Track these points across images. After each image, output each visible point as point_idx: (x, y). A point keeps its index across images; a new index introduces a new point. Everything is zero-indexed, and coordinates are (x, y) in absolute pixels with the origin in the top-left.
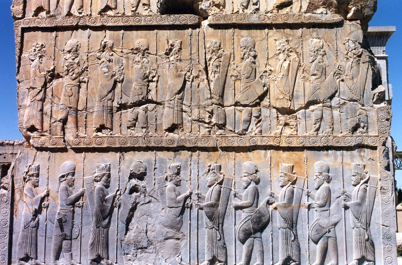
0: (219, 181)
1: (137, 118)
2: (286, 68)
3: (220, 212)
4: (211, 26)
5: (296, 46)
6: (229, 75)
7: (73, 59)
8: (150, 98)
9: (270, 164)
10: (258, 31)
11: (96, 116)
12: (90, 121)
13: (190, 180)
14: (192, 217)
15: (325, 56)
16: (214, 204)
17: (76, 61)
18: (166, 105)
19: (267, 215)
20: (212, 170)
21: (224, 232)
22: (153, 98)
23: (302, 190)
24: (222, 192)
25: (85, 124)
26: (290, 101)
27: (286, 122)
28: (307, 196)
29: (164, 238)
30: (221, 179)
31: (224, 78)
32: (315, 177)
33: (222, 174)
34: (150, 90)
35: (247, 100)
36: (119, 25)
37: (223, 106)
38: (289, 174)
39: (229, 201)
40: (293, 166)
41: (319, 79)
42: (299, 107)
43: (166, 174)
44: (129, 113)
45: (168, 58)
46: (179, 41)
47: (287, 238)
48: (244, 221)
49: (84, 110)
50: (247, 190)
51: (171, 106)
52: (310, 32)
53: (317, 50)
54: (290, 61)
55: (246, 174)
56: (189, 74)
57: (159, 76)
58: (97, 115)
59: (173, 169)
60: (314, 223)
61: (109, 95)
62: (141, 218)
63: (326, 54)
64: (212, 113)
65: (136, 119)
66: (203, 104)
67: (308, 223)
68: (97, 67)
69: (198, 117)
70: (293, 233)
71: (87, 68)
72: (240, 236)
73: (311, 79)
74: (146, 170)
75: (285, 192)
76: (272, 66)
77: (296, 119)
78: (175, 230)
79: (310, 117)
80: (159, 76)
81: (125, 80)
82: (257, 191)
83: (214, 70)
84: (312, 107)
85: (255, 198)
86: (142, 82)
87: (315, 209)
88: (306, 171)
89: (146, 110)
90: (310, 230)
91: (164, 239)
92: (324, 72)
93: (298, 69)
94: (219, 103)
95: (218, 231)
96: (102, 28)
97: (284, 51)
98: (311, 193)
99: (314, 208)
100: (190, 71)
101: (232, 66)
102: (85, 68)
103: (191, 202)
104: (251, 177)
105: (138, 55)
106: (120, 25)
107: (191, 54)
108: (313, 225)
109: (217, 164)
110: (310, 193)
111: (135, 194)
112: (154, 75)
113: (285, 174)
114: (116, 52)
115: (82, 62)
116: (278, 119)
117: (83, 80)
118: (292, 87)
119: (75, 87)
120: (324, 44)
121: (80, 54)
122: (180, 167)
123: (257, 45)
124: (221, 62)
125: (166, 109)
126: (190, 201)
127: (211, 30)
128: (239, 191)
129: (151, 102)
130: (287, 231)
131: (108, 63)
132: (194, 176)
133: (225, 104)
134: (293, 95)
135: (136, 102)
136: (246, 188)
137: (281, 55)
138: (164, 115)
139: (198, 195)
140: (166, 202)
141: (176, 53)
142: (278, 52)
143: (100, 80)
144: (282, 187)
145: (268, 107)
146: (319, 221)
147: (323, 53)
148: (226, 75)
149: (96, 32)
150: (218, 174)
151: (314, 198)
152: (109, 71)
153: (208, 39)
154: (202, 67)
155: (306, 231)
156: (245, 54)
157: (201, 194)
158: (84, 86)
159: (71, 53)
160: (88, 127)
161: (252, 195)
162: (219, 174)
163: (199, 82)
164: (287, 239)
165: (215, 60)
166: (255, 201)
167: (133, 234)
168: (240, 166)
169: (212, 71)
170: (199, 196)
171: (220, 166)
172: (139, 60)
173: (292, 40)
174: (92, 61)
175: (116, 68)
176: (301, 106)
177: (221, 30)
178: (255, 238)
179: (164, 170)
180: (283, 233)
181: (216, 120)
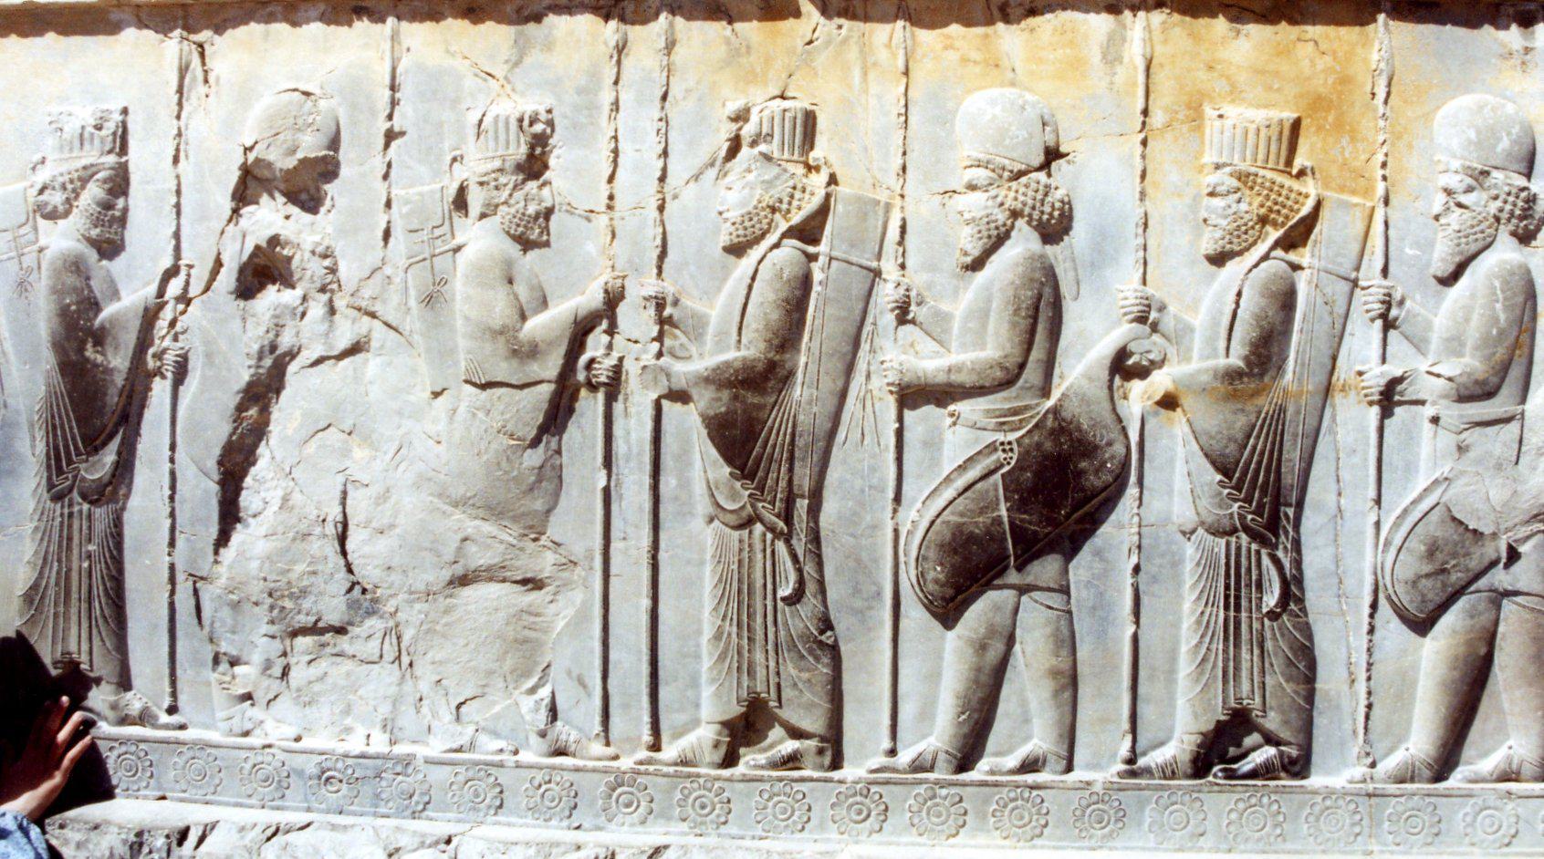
0: (796, 218)
3: (801, 418)
9: (1140, 105)
13: (610, 207)
14: (620, 447)
16: (760, 367)
19: (1110, 444)
20: (754, 144)
21: (827, 551)
23: (1346, 287)
24: (816, 288)
28: (1379, 323)
29: (446, 574)
30: (811, 204)
32: (1442, 198)
33: (817, 169)
38: (1269, 174)
39: (865, 346)
40: (1296, 126)
43: (461, 173)
47: (1238, 598)
48: (961, 482)
50: (981, 277)
55: (981, 175)
59: (502, 136)
60: (1415, 502)
62: (312, 447)
67: (1378, 501)
70: (1277, 563)
72: (931, 575)
74: (334, 143)
75: (1239, 294)
78: (516, 530)
82: (1047, 291)
85: (1032, 332)
87: (1429, 411)
88: (1380, 158)
90: (1387, 543)
91: (451, 583)
95: (788, 542)
98: (1408, 303)
99: (1422, 403)
103: (615, 355)
104: (1013, 195)
108: (1406, 511)
109: (787, 104)
110: (1401, 303)
111: (272, 297)
113: (1242, 177)
122: (550, 123)
126: (610, 347)
128: (930, 286)
130: (1239, 548)
132: (636, 183)
136: (977, 265)
139: (660, 306)
140: (453, 351)
144: (1219, 259)
146: (1451, 492)
150: (792, 168)
151: (1426, 341)
155: (1361, 554)
157: (676, 303)
161: (1016, 312)
162: (800, 170)
164: (1233, 601)
166: (1037, 354)
167: (262, 547)
168: (945, 119)
170: (667, 312)
171: (810, 120)
178: (1023, 590)
179: (447, 145)
180: (1208, 563)
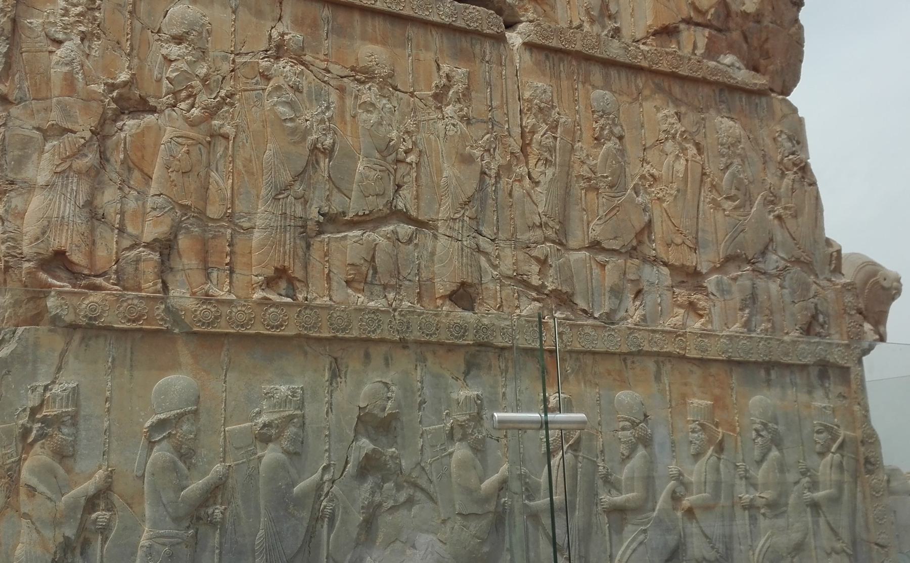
8: (401, 205)
18: (441, 231)
22: (408, 206)
35: (615, 238)
44: (349, 242)
45: (440, 108)
51: (455, 234)
54: (687, 160)
66: (524, 237)
69: (514, 271)
81: (337, 147)
100: (492, 150)
105: (367, 86)
107: (491, 108)
112: (411, 147)
114: (311, 68)
127: (527, 59)
138: (436, 258)
156: (602, 129)
160: (237, 272)
169: (539, 159)
173: (686, 114)
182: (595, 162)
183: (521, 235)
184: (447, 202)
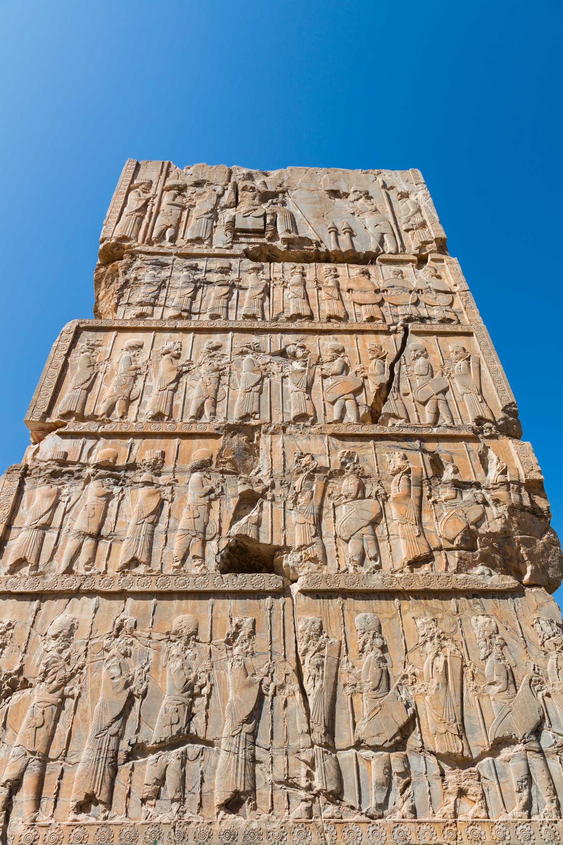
1: (164, 778)
2: (441, 670)
4: (304, 592)
5: (452, 629)
6: (340, 684)
7: (60, 652)
10: (384, 602)
11: (81, 771)
12: (68, 785)
15: (505, 647)
17: (65, 655)
18: (223, 747)
25: (55, 791)
26: (461, 738)
27: (462, 786)
31: (331, 689)
34: (194, 715)
35: (378, 735)
36: (149, 590)
37: (335, 751)
41: (506, 693)
42: (480, 752)
44: (148, 765)
46: (249, 620)
49: (61, 758)
52: (470, 604)
53: (490, 637)
54: (446, 657)
56: (267, 680)
57: (212, 685)
58: (84, 770)
61: (114, 725)
63: (506, 644)
64: (312, 764)
65: (161, 781)
66: (293, 744)
68: (100, 666)
71: (82, 668)
73: (490, 692)
76: (415, 665)
77: (479, 780)
79: (505, 774)
80: (212, 685)
81: (149, 692)
83: (313, 673)
84: (506, 753)
86: (180, 698)
89: (184, 760)
92: (510, 678)
93: (462, 672)
94: (325, 743)
96: (122, 595)
97: (432, 638)
100: (270, 674)
101: (344, 667)
102: (79, 668)
105: (177, 643)
106: (152, 590)
114: (139, 638)
115: (74, 657)
116: (443, 781)
117: (70, 693)
118: (459, 708)
119: (53, 706)
120: (499, 625)
121: (74, 642)
123: (385, 627)
124: (323, 657)
125: (223, 754)
129: (195, 739)
131: (122, 658)
133: (338, 745)
134: (463, 725)
135: (164, 741)
137: (429, 644)
141: (245, 641)
142: (421, 640)
143: (101, 692)
145: (421, 751)
147: (502, 642)
148: (336, 684)
149: (109, 602)
152: (121, 673)
153: (299, 616)
154: (291, 666)
156: (365, 643)
158: (69, 703)
159: (58, 639)
163: (285, 696)
165: (313, 655)
172: (179, 654)
174: (92, 655)
175: (135, 669)
176: (482, 749)
177: (321, 600)
181: (321, 781)
182: (360, 670)
183: (292, 742)
184: (228, 722)
